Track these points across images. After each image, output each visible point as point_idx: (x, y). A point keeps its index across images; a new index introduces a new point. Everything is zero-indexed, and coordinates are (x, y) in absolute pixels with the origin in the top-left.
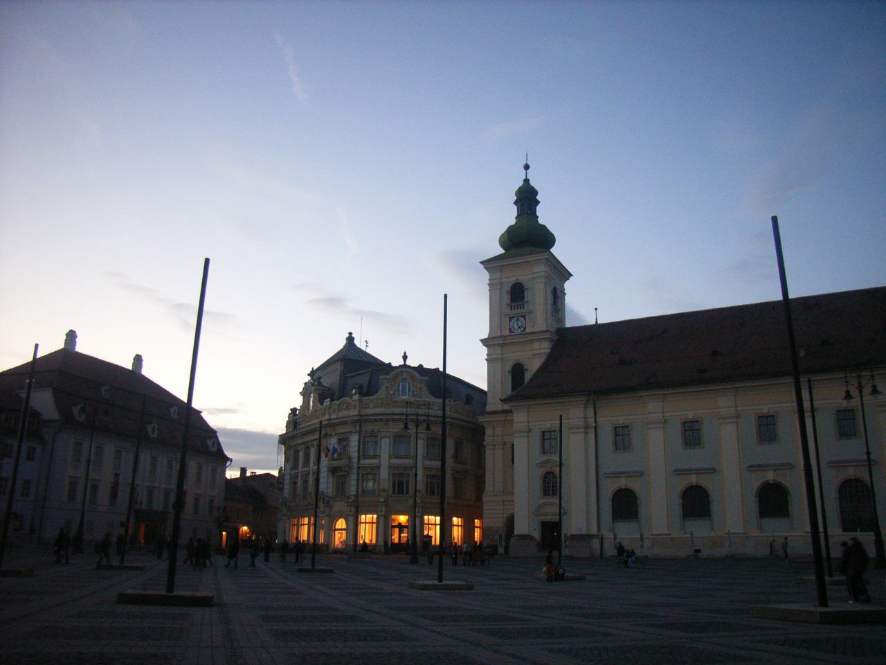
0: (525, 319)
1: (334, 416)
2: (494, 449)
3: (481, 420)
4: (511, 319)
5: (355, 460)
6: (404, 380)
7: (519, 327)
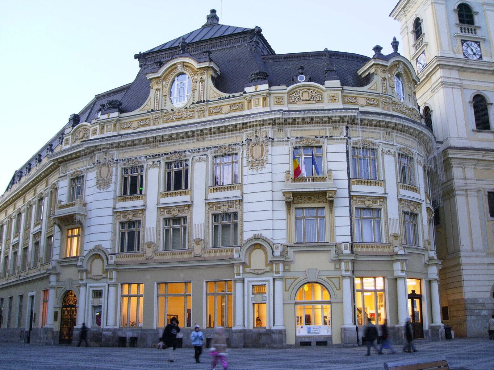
0: (479, 46)
2: (467, 196)
3: (450, 156)
4: (463, 42)
7: (474, 54)
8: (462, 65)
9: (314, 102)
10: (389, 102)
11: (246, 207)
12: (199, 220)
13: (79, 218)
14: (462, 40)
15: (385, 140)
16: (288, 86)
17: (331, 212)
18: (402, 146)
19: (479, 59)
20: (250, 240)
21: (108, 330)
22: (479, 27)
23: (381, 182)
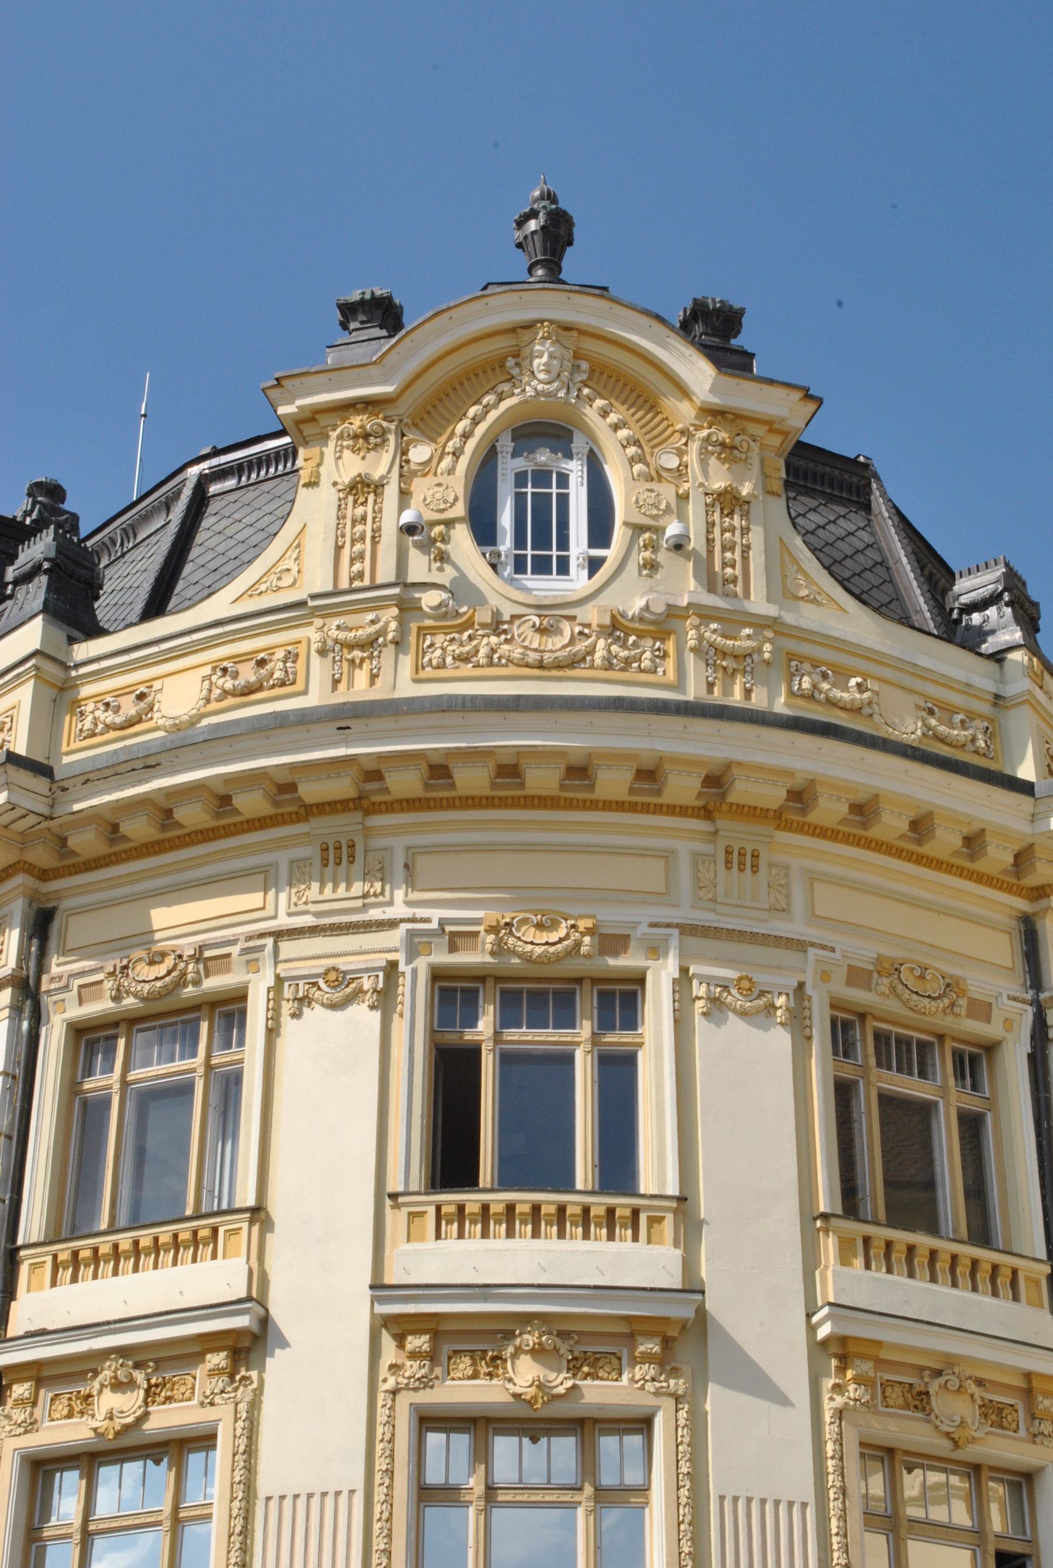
10: (382, 632)
23: (225, 1225)
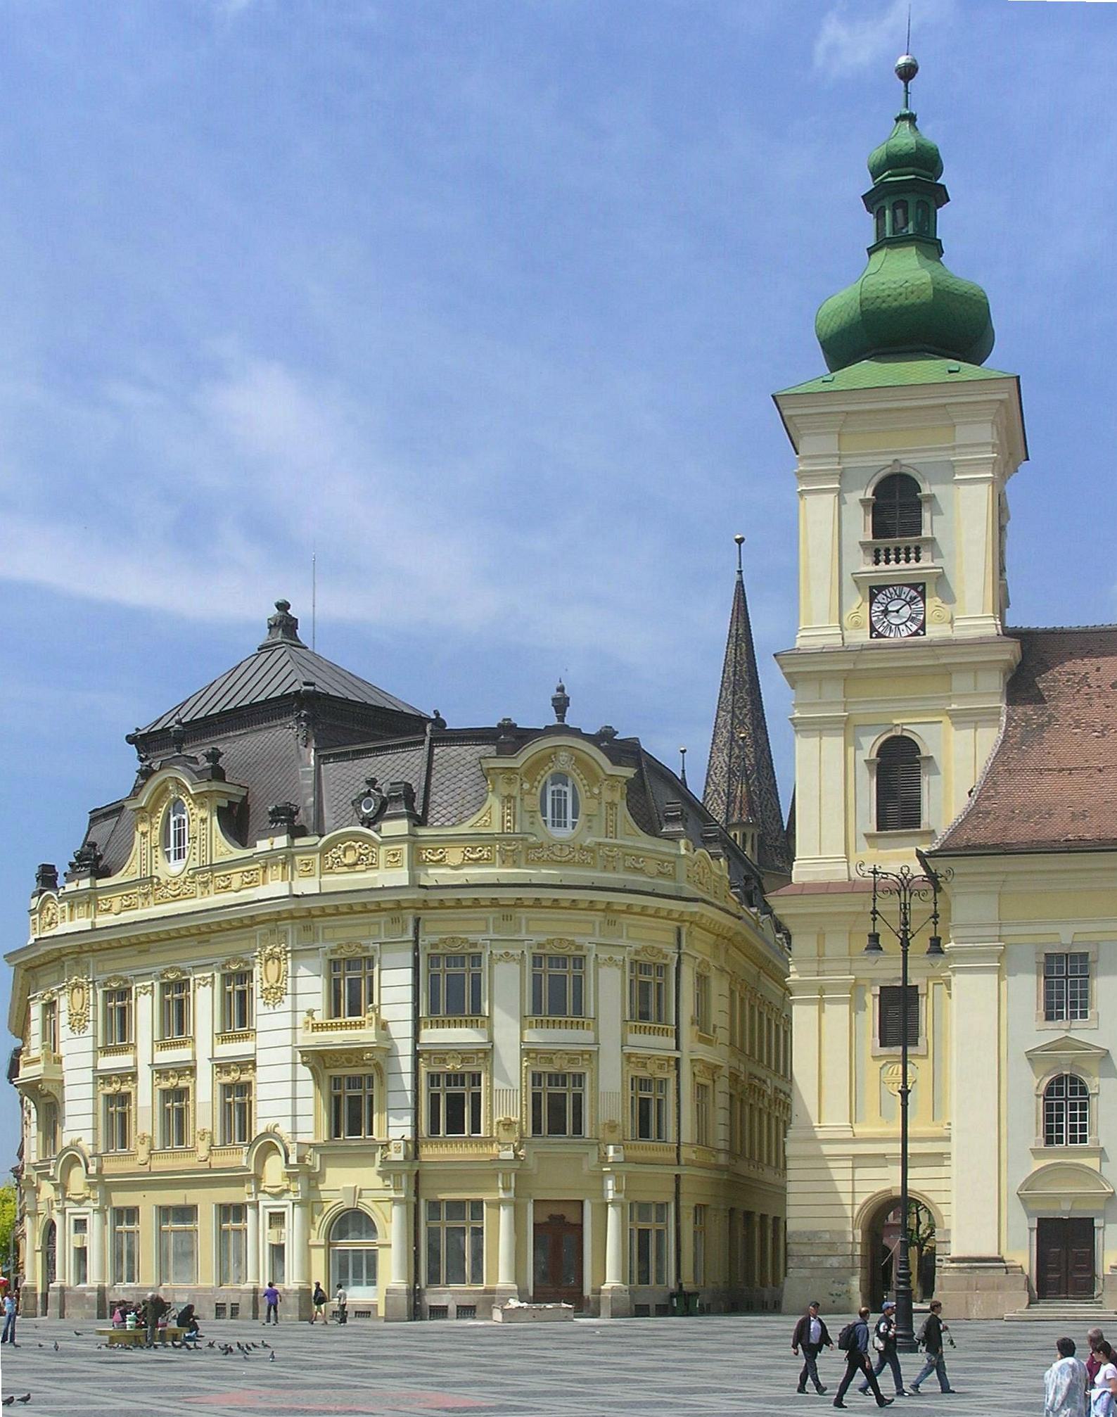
1: (306, 886)
4: (874, 592)
5: (402, 1031)
6: (560, 778)
8: (852, 667)
9: (363, 867)
11: (261, 1075)
12: (205, 1093)
13: (47, 1087)
14: (871, 588)
15: (498, 933)
16: (321, 836)
17: (382, 1083)
18: (543, 939)
19: (916, 634)
20: (263, 1135)
21: (91, 1289)
22: (932, 541)
23: (480, 1019)
